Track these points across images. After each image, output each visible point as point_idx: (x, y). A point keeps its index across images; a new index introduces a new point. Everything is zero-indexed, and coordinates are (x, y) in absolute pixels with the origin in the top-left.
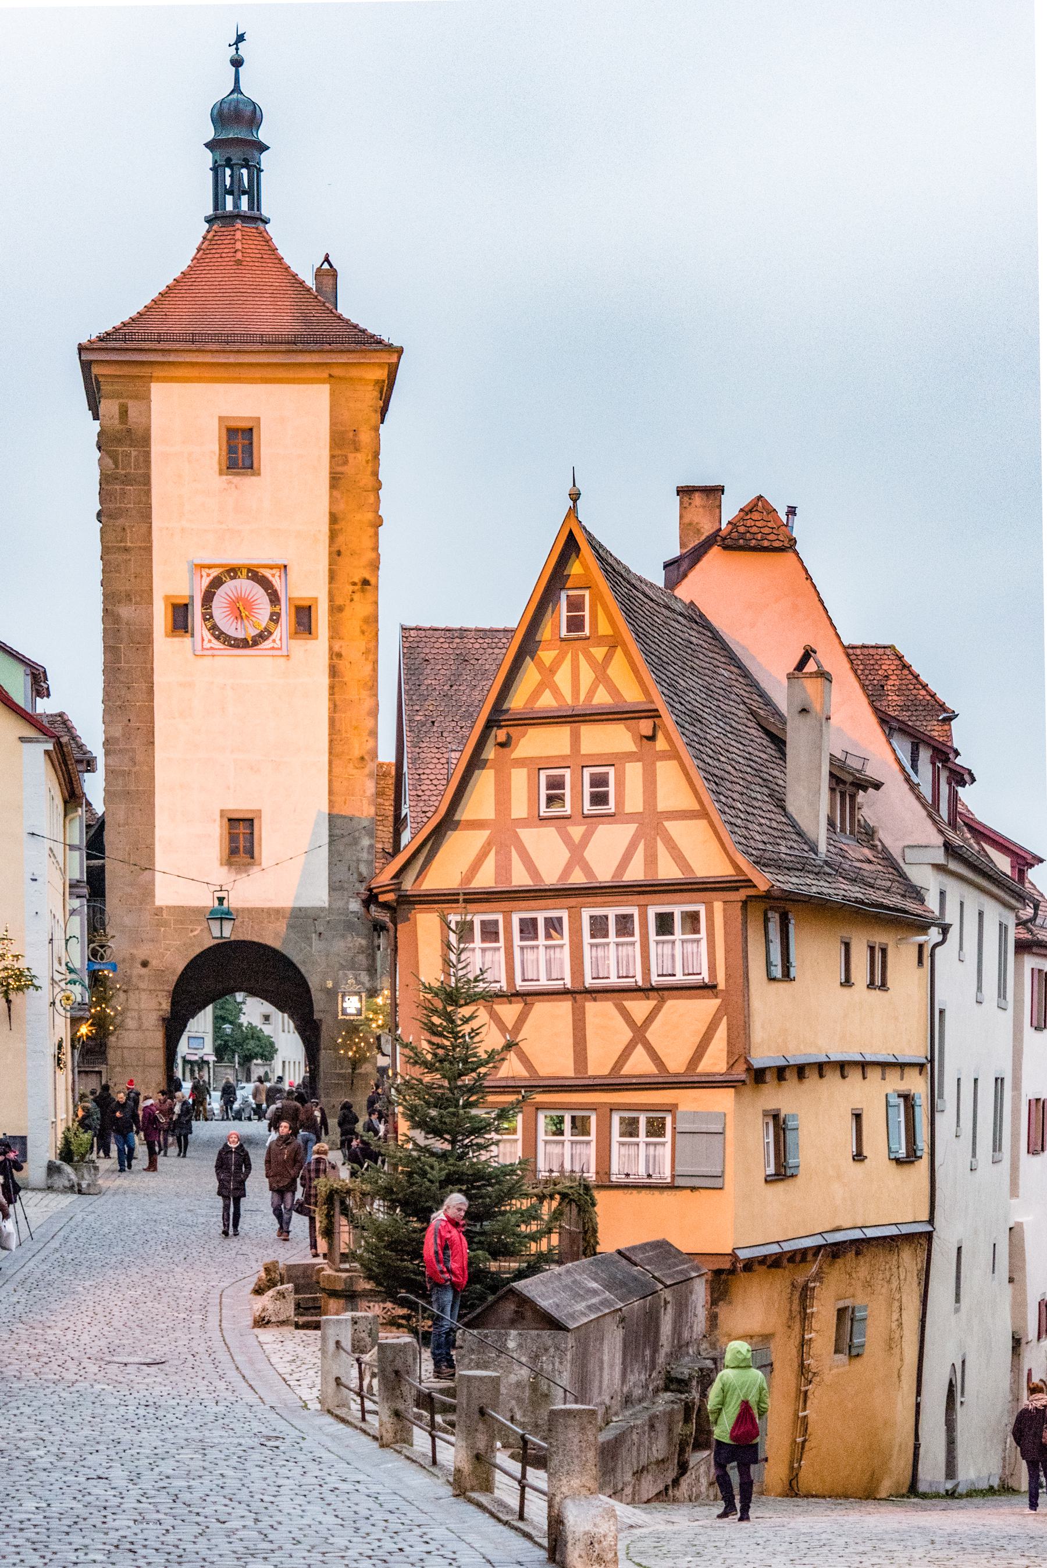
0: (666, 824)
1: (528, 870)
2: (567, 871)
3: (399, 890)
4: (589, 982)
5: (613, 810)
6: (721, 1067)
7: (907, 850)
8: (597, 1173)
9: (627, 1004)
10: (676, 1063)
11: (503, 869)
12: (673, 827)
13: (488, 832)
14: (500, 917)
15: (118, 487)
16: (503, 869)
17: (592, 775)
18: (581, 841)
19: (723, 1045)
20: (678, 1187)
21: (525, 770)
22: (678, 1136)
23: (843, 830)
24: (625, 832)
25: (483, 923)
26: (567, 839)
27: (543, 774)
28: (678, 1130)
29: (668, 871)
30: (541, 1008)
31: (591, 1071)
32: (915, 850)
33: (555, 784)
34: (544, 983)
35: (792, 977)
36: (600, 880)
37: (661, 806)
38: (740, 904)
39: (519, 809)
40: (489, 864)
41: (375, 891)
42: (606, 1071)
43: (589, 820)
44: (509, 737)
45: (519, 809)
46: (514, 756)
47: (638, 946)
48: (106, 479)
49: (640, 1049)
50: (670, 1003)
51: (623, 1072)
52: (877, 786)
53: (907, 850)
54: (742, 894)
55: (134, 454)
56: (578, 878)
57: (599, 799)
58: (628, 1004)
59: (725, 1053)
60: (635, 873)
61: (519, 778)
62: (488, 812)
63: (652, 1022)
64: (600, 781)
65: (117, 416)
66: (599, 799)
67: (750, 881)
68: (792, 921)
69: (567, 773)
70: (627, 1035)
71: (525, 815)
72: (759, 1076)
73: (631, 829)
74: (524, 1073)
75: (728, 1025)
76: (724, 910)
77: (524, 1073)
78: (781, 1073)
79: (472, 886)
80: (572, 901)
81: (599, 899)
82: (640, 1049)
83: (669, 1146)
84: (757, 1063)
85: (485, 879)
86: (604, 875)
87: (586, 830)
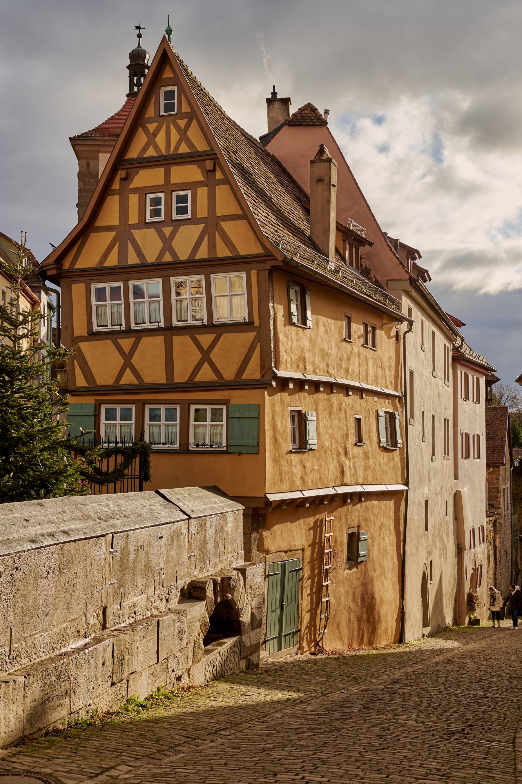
0: (221, 223)
1: (138, 256)
2: (161, 254)
3: (61, 268)
4: (175, 323)
5: (190, 217)
6: (257, 376)
7: (389, 282)
8: (180, 444)
9: (197, 336)
10: (229, 374)
11: (123, 254)
12: (225, 225)
13: (115, 233)
14: (120, 284)
15: (85, 194)
16: (123, 254)
17: (177, 196)
18: (170, 236)
19: (258, 361)
20: (230, 453)
21: (138, 194)
22: (229, 419)
23: (351, 264)
24: (197, 229)
25: (112, 288)
26: (161, 235)
27: (149, 197)
28: (230, 416)
29: (222, 251)
30: (146, 341)
31: (176, 381)
32: (394, 282)
33: (156, 202)
34: (148, 325)
35: (308, 326)
36: (181, 259)
37: (218, 213)
38: (267, 271)
39: (133, 219)
40: (115, 251)
41: (44, 268)
42: (185, 380)
43: (174, 223)
44: (127, 173)
45: (133, 219)
46: (132, 186)
47: (204, 300)
48: (79, 191)
49: (206, 365)
50: (224, 335)
51: (196, 380)
52: (371, 244)
53: (389, 282)
54: (268, 265)
55: (92, 181)
56: (167, 258)
57: (182, 211)
58: (197, 336)
59: (259, 366)
60: (202, 254)
61: (134, 200)
62: (115, 221)
63: (213, 348)
64: (182, 199)
65: (85, 166)
66: (182, 211)
67: (273, 256)
68: (308, 292)
69: (162, 195)
70: (199, 356)
71: (136, 222)
72: (283, 383)
73: (201, 227)
74: (136, 382)
75: (261, 348)
76: (258, 276)
77: (136, 382)
78: (300, 384)
79: (104, 265)
80: (165, 273)
81: (181, 271)
82: (206, 365)
83: (225, 427)
84: (281, 373)
85: (112, 261)
86: (184, 256)
87: (173, 229)
